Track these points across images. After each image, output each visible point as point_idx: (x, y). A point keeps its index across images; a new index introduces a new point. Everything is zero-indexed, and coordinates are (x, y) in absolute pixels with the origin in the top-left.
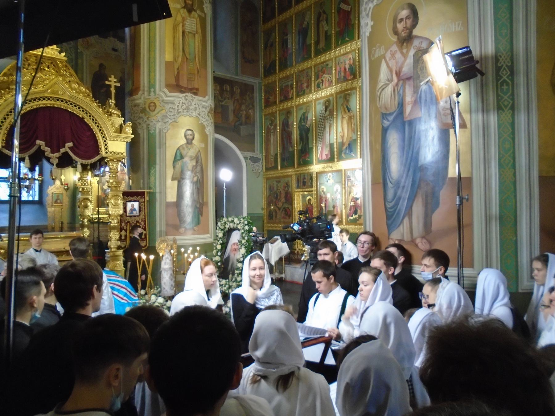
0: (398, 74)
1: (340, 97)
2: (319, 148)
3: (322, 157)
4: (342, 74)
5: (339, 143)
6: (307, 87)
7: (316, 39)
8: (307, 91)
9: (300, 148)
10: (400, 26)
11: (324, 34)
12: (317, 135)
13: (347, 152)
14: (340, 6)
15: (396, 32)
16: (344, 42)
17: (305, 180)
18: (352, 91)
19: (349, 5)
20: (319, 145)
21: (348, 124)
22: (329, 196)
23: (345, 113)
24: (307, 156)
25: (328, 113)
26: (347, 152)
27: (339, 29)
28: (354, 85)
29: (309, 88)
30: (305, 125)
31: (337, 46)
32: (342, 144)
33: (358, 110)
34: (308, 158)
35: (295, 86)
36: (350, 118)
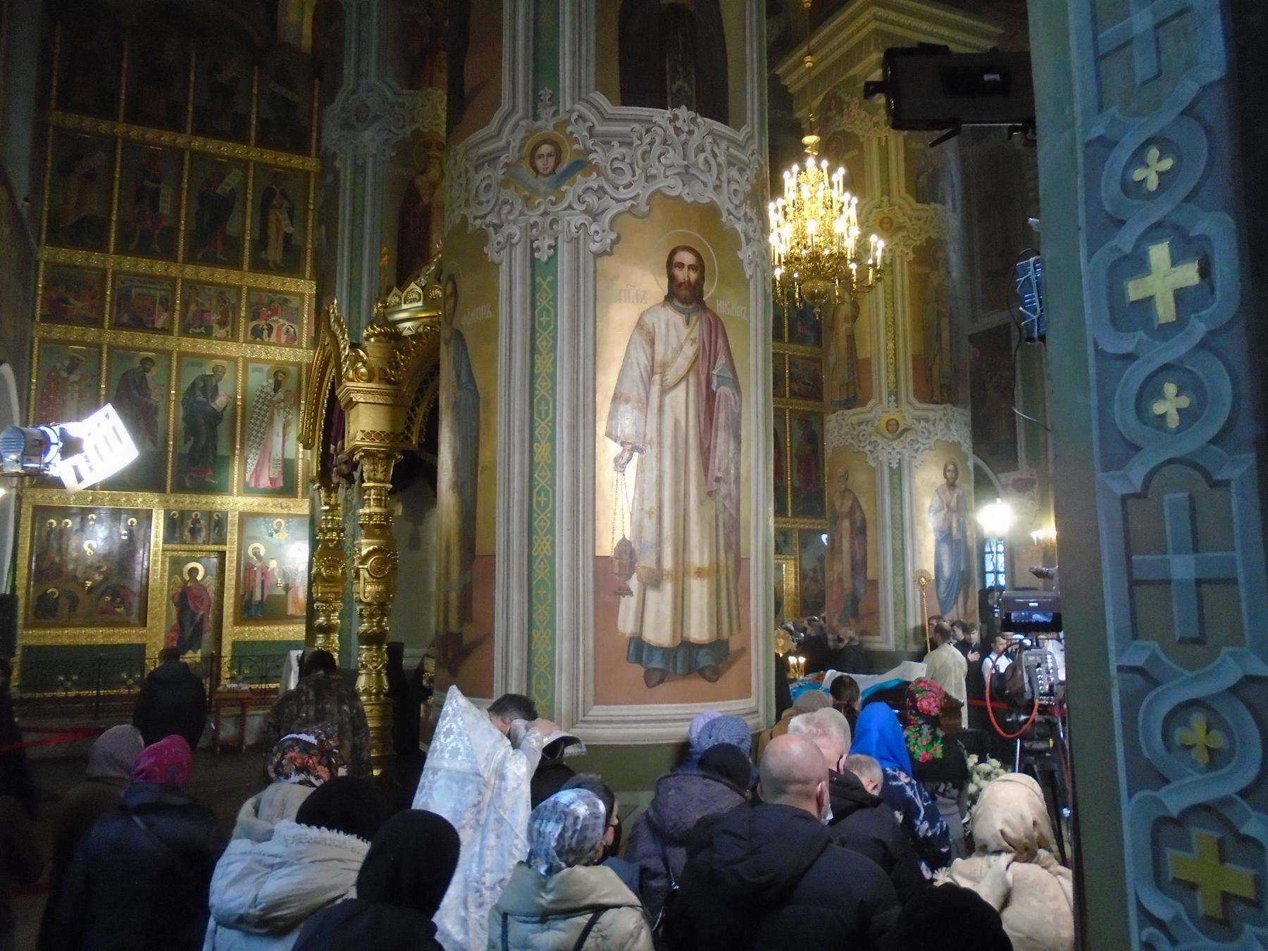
0: (948, 506)
2: (249, 461)
3: (257, 481)
6: (222, 324)
7: (257, 237)
8: (218, 332)
9: (186, 449)
10: (949, 474)
11: (281, 239)
12: (247, 437)
15: (945, 477)
17: (198, 526)
20: (251, 456)
22: (273, 564)
24: (210, 472)
25: (280, 395)
29: (229, 328)
30: (207, 404)
34: (213, 477)
35: (178, 307)
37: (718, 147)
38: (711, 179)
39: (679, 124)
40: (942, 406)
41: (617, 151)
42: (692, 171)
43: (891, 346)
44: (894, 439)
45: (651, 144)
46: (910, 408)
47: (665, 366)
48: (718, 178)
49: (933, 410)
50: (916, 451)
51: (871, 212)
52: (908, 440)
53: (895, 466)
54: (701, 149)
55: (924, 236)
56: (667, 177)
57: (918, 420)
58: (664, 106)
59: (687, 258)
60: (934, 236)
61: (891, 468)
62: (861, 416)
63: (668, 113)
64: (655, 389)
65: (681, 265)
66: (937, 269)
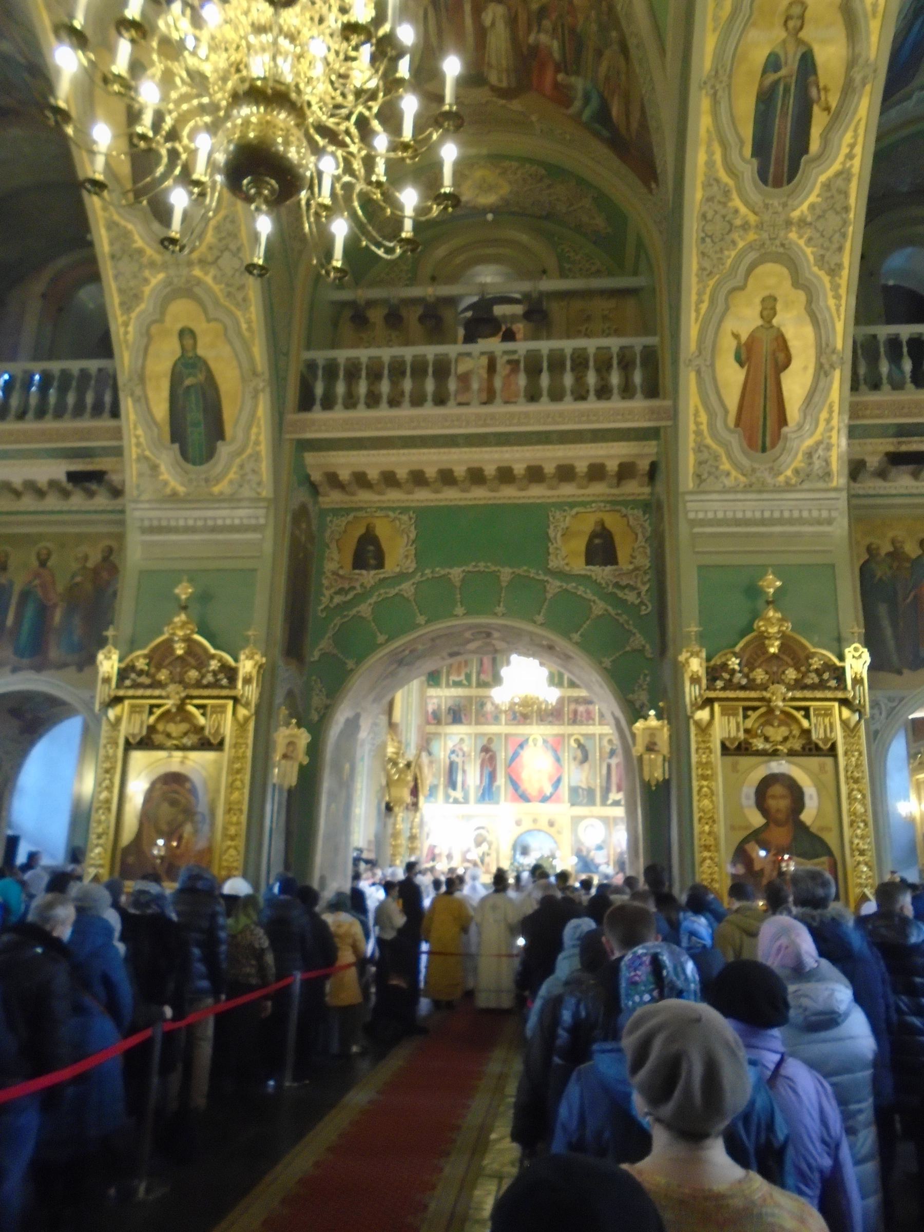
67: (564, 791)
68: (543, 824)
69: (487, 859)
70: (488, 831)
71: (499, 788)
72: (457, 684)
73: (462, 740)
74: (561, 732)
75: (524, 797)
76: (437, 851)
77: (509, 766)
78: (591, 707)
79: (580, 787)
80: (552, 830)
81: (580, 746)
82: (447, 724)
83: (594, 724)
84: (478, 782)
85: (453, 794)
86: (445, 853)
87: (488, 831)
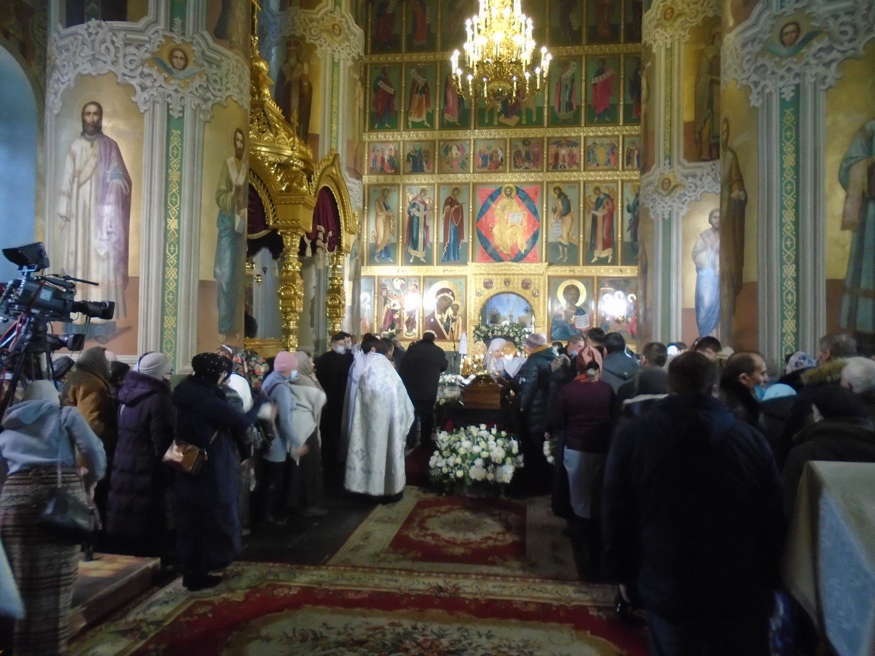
1: (375, 191)
4: (379, 164)
5: (371, 244)
13: (383, 255)
14: (379, 84)
16: (382, 128)
18: (393, 188)
19: (391, 87)
21: (385, 224)
23: (382, 210)
26: (383, 255)
27: (376, 110)
28: (399, 181)
31: (372, 129)
32: (376, 246)
33: (401, 211)
36: (388, 218)
37: (116, 36)
38: (109, 58)
39: (90, 30)
40: (711, 163)
41: (65, 54)
42: (97, 56)
43: (668, 117)
44: (667, 195)
45: (76, 47)
46: (680, 168)
47: (80, 172)
48: (116, 56)
49: (701, 167)
50: (683, 203)
51: (659, 7)
52: (677, 194)
53: (666, 217)
54: (103, 41)
55: (701, 17)
56: (83, 63)
57: (686, 177)
58: (82, 22)
59: (92, 108)
60: (711, 14)
61: (664, 219)
62: (649, 179)
63: (85, 26)
64: (75, 186)
65: (89, 113)
66: (713, 43)
67: (542, 247)
68: (517, 285)
69: (452, 325)
70: (453, 295)
71: (467, 244)
72: (417, 126)
73: (423, 190)
74: (539, 180)
75: (494, 255)
76: (396, 316)
77: (478, 220)
78: (575, 150)
79: (560, 243)
80: (528, 292)
81: (561, 195)
82: (405, 174)
83: (580, 171)
84: (441, 240)
85: (413, 253)
86: (406, 318)
87: (453, 295)
